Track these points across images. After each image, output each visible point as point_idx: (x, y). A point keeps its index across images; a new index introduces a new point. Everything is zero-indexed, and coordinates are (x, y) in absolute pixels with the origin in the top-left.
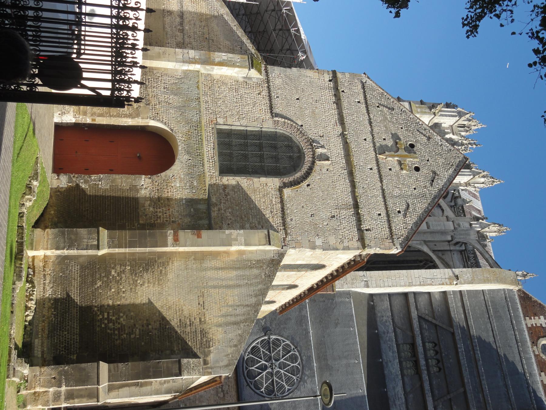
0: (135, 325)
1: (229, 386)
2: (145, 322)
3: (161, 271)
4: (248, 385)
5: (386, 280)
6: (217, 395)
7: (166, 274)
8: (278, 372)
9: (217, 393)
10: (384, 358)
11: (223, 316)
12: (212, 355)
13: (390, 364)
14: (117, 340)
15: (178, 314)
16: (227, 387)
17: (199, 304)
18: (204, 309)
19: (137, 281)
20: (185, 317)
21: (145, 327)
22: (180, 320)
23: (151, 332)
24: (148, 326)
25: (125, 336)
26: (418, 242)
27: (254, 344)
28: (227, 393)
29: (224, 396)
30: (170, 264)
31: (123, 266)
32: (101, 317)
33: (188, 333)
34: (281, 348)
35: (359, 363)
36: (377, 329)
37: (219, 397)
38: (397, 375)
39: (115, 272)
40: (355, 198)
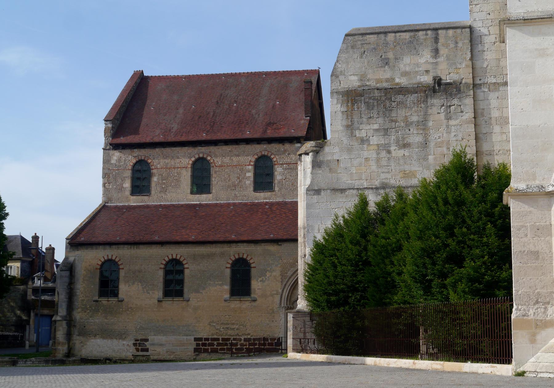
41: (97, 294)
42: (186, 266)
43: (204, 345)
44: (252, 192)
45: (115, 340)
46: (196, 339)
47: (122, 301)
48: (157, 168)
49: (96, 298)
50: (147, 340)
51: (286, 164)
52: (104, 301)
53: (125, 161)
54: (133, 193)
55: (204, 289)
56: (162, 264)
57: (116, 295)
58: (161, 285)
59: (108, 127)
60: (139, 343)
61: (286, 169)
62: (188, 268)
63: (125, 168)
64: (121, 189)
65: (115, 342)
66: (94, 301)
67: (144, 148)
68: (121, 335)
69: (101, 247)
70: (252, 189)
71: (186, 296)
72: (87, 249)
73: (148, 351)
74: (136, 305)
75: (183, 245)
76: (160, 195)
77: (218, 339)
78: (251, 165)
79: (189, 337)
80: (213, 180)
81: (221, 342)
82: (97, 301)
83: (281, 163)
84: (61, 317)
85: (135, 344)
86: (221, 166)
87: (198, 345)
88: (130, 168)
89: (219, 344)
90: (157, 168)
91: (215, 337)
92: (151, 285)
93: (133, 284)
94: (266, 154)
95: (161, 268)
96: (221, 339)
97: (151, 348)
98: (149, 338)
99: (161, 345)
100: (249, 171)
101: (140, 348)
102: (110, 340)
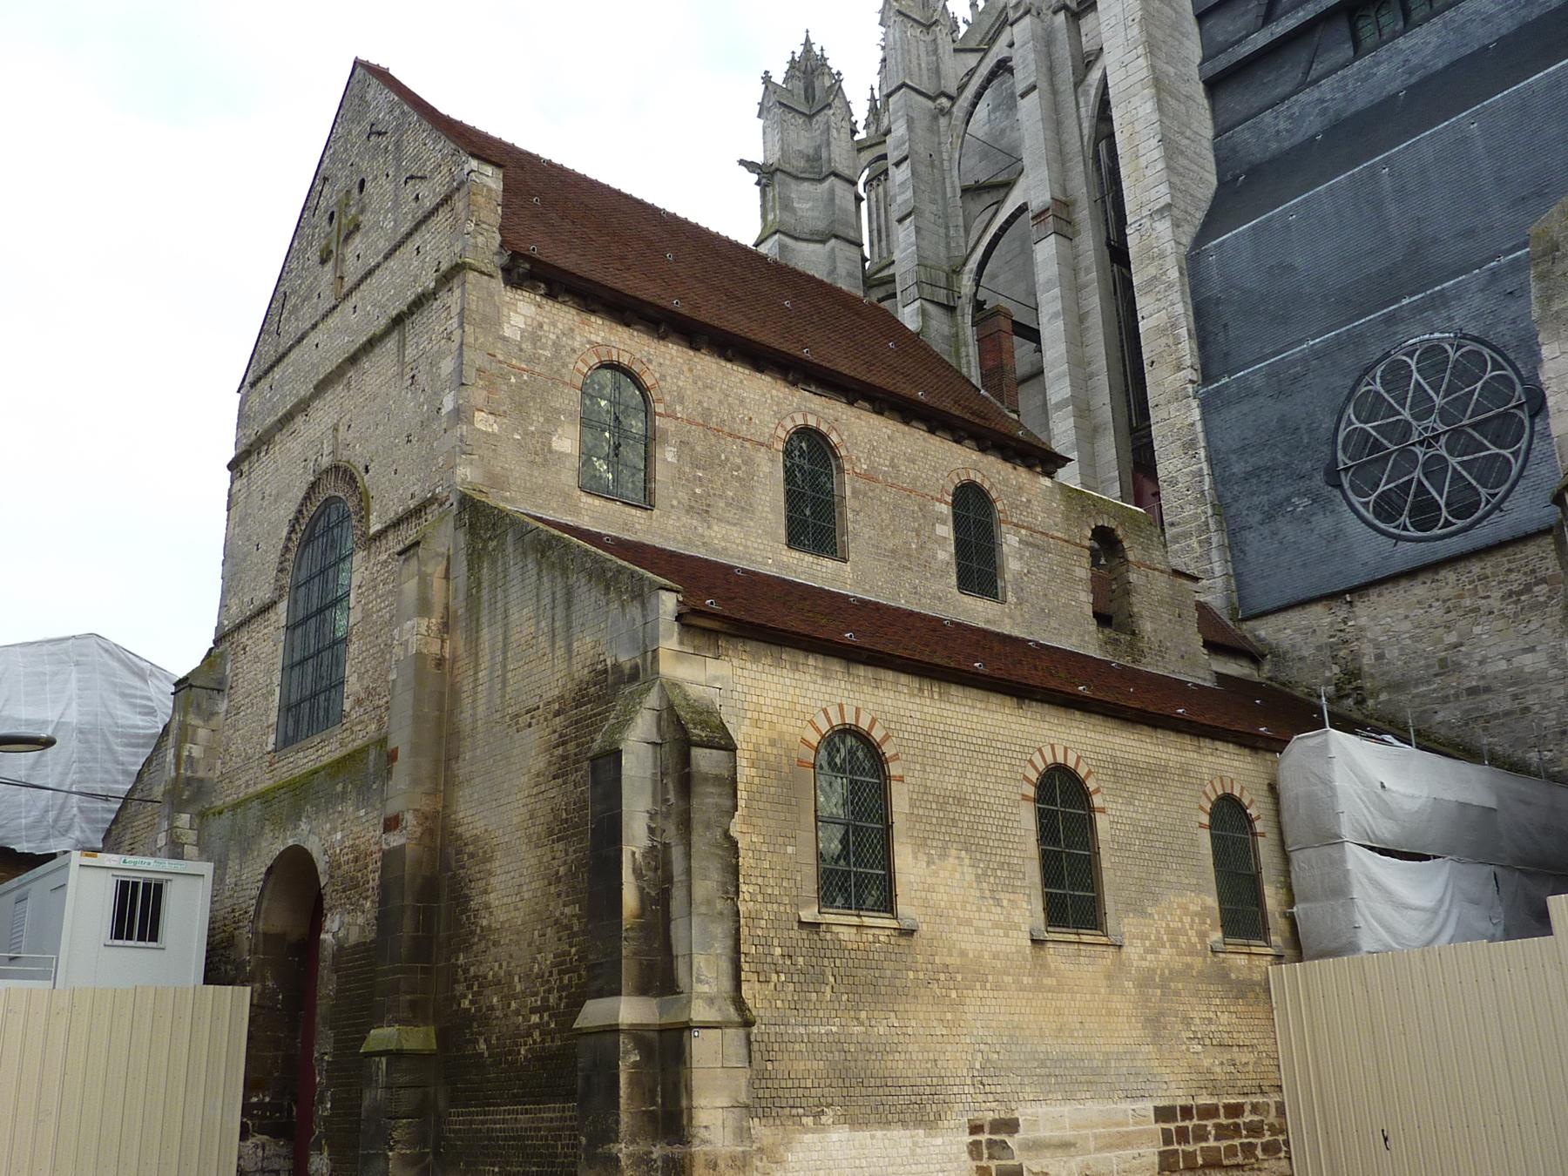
0: (556, 922)
1: (1510, 570)
2: (552, 889)
3: (471, 856)
4: (1498, 507)
5: (1143, 162)
6: (1545, 604)
7: (476, 839)
8: (1444, 416)
9: (1533, 607)
10: (1391, 88)
12: (623, 659)
13: (1415, 60)
16: (1513, 576)
17: (530, 725)
21: (562, 887)
24: (558, 880)
26: (1082, 100)
27: (1370, 516)
28: (1533, 571)
29: (1544, 581)
30: (459, 830)
32: (536, 1034)
33: (578, 745)
34: (1367, 427)
35: (1387, 162)
36: (1312, 138)
37: (1551, 598)
38: (1445, 25)
39: (465, 997)
41: (810, 887)
42: (1097, 801)
43: (1183, 1135)
44: (955, 590)
45: (897, 1133)
46: (1163, 1114)
47: (909, 933)
48: (671, 415)
49: (809, 914)
50: (1011, 1126)
53: (557, 345)
54: (591, 487)
55: (1156, 901)
56: (1026, 778)
57: (887, 904)
58: (1032, 871)
59: (490, 189)
60: (991, 1143)
61: (1027, 544)
62: (1103, 810)
64: (545, 456)
67: (628, 325)
69: (811, 661)
70: (953, 580)
71: (1111, 922)
72: (756, 659)
74: (963, 954)
75: (1078, 715)
77: (1209, 1112)
79: (1139, 1105)
80: (850, 515)
81: (1223, 1121)
82: (816, 925)
84: (711, 1001)
86: (869, 477)
87: (1167, 1139)
89: (1222, 1131)
90: (671, 415)
91: (1205, 1100)
92: (1001, 866)
93: (944, 856)
95: (1025, 797)
96: (1222, 1111)
98: (1023, 1113)
99: (1065, 1145)
100: (944, 523)
101: (993, 1164)
102: (879, 1134)
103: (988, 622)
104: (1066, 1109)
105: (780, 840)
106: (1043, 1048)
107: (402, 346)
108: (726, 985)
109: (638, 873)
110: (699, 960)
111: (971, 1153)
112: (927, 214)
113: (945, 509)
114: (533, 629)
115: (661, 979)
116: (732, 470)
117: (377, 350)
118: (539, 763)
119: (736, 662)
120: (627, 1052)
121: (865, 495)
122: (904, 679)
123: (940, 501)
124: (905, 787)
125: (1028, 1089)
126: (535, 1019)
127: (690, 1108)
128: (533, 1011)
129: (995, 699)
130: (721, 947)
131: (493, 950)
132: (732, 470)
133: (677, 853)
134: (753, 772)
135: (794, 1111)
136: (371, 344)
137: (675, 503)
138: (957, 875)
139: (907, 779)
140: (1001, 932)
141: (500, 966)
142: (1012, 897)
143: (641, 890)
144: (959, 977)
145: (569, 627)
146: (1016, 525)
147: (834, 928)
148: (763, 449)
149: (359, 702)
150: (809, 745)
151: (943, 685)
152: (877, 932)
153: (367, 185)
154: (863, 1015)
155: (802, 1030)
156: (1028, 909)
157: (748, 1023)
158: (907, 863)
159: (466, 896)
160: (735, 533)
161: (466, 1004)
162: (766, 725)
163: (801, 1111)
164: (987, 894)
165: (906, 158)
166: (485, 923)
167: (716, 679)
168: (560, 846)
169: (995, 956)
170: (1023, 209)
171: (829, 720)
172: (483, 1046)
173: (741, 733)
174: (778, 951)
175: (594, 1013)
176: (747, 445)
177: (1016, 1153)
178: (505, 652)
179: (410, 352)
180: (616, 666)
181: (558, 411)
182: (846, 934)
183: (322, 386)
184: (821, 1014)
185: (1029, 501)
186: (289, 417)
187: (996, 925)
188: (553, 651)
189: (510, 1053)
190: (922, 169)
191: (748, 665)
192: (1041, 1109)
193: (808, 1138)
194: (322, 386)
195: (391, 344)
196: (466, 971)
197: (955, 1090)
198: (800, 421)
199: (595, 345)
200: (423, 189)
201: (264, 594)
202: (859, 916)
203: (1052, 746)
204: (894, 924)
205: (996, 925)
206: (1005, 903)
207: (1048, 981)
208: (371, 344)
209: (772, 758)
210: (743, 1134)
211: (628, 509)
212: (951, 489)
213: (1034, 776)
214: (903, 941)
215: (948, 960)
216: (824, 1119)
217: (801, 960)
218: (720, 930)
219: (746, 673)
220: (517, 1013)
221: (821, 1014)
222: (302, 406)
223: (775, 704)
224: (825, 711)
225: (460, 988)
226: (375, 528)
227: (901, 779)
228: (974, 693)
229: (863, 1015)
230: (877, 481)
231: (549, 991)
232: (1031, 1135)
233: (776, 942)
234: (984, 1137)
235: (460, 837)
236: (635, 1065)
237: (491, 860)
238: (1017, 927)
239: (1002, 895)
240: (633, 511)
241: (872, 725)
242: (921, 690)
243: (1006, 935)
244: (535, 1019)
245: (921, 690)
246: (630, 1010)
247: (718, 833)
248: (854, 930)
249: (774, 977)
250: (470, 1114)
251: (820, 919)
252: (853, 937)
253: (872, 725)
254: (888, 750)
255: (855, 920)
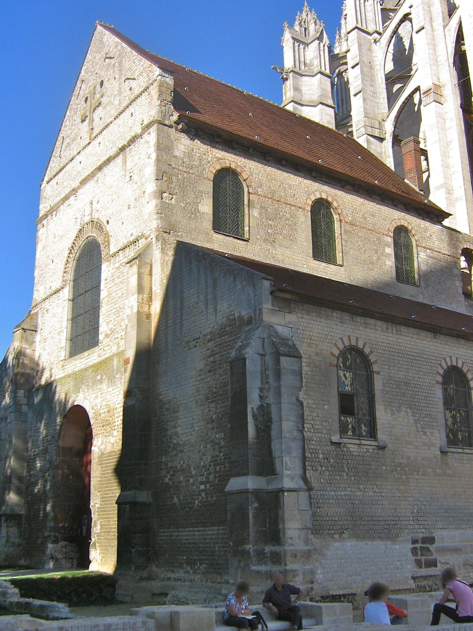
2: (210, 426)
11: (207, 307)
12: (244, 313)
14: (225, 467)
15: (203, 377)
17: (195, 346)
18: (200, 338)
19: (174, 444)
20: (206, 365)
22: (209, 372)
23: (218, 416)
25: (221, 455)
31: (161, 466)
32: (203, 494)
33: (221, 356)
39: (166, 476)
40: (117, 155)
47: (382, 448)
48: (256, 194)
49: (336, 438)
50: (431, 540)
51: (430, 249)
52: (352, 446)
56: (438, 373)
57: (373, 434)
59: (167, 84)
60: (422, 548)
63: (202, 173)
64: (195, 213)
65: (379, 545)
66: (333, 443)
68: (388, 531)
72: (308, 313)
73: (436, 566)
74: (409, 458)
75: (462, 341)
76: (264, 245)
78: (390, 237)
82: (339, 444)
83: (424, 245)
84: (292, 479)
85: (414, 551)
88: (212, 177)
90: (256, 194)
93: (399, 411)
94: (406, 225)
95: (438, 382)
97: (441, 558)
98: (437, 534)
99: (457, 550)
100: (389, 246)
101: (423, 558)
102: (370, 543)
103: (411, 296)
104: (457, 532)
105: (322, 402)
106: (446, 503)
107: (125, 162)
108: (299, 471)
109: (254, 416)
110: (286, 459)
111: (412, 553)
112: (369, 92)
113: (390, 240)
114: (196, 299)
115: (267, 467)
116: (286, 220)
117: (111, 164)
118: (200, 365)
119: (299, 315)
120: (252, 502)
121: (351, 233)
122: (379, 323)
123: (387, 235)
124: (380, 377)
125: (439, 523)
126: (202, 487)
127: (284, 528)
128: (202, 483)
129: (423, 333)
130: (296, 453)
131: (180, 455)
132: (286, 220)
133: (273, 409)
134: (308, 369)
135: (330, 532)
136: (109, 161)
137: (258, 237)
138: (406, 420)
139: (381, 373)
140: (427, 448)
141: (184, 462)
142: (432, 431)
143: (256, 426)
144: (407, 469)
145: (215, 298)
146: (424, 248)
147: (348, 445)
148: (301, 210)
149: (107, 336)
150: (334, 356)
151: (398, 326)
152: (368, 447)
153: (105, 83)
154: (362, 486)
155: (333, 493)
156: (439, 438)
157: (310, 489)
158: (382, 415)
159: (165, 429)
160: (288, 252)
161: (167, 480)
162: (314, 346)
163: (333, 532)
164: (420, 429)
165: (357, 64)
166: (175, 442)
167: (290, 323)
168: (213, 405)
169: (424, 459)
170: (418, 89)
171: (344, 344)
172: (176, 500)
173: (303, 349)
174: (321, 456)
175: (234, 484)
176: (292, 208)
177: (434, 553)
178: (181, 311)
179: (129, 164)
180: (240, 317)
181: (201, 192)
182: (353, 448)
183: (84, 182)
184: (342, 486)
185: (431, 236)
186: (66, 198)
187: (424, 444)
188: (207, 310)
189: (190, 503)
190: (366, 69)
191: (305, 316)
192: (445, 533)
193: (337, 544)
194: (84, 182)
195: (119, 159)
196: (166, 464)
197: (405, 523)
198: (318, 196)
199: (219, 159)
200: (133, 84)
201: (57, 284)
202: (359, 440)
203: (451, 357)
204: (375, 443)
205: (424, 444)
206: (428, 434)
207: (448, 471)
208: (109, 161)
209: (317, 362)
210: (307, 541)
211: (236, 240)
212: (393, 230)
213: (442, 372)
214: (380, 452)
215: (401, 461)
216: (344, 535)
217: (332, 460)
218: (295, 446)
219: (304, 320)
220: (193, 484)
221: (342, 486)
222: (74, 191)
223: (320, 335)
224: (342, 339)
225: (164, 473)
226: (113, 250)
227: (378, 373)
228: (412, 330)
229: (362, 486)
230: (357, 226)
231: (209, 474)
232: (440, 545)
233: (320, 451)
234: (418, 546)
235: (162, 401)
236: (256, 508)
237: (177, 411)
238: (434, 445)
239: (427, 430)
240: (239, 241)
241: (364, 346)
242: (387, 329)
243: (429, 449)
244: (202, 487)
245: (387, 329)
246: (251, 482)
247: (294, 399)
248: (357, 446)
249: (320, 468)
250: (170, 532)
251: (341, 441)
252: (356, 450)
253: (364, 346)
254: (372, 358)
255: (357, 442)
